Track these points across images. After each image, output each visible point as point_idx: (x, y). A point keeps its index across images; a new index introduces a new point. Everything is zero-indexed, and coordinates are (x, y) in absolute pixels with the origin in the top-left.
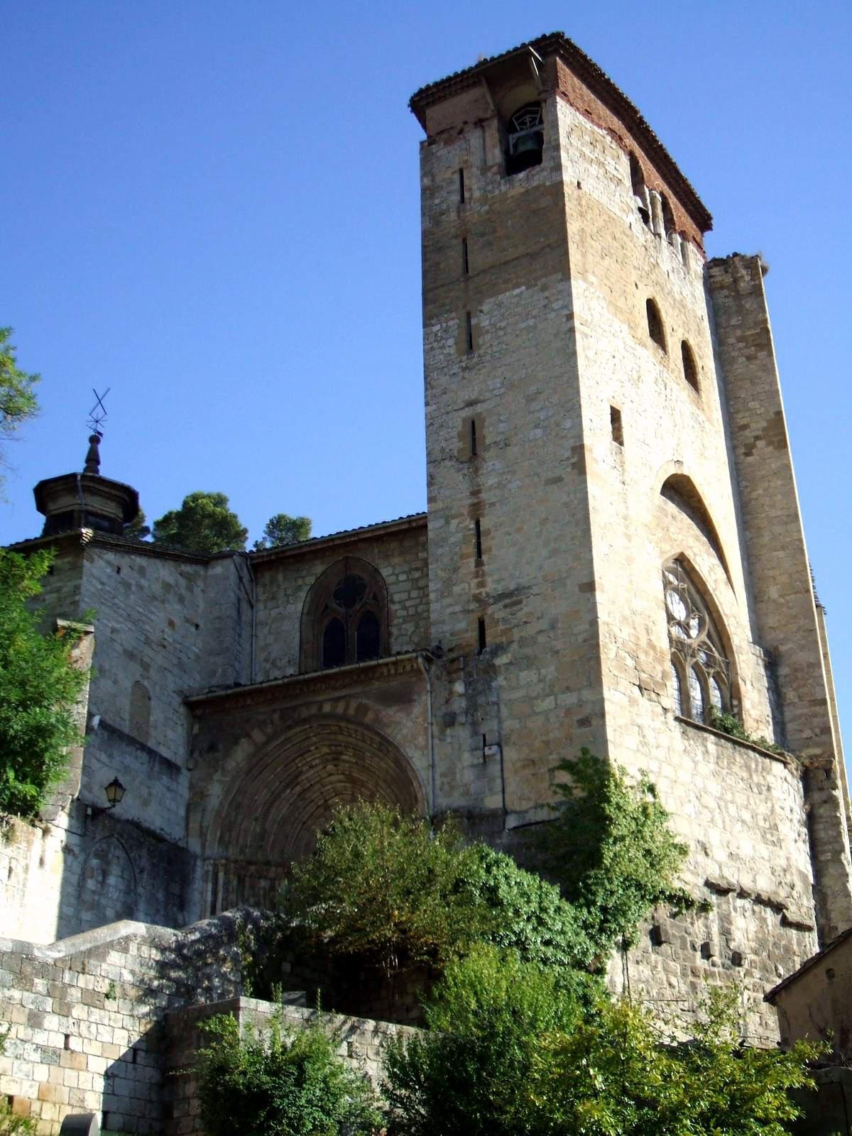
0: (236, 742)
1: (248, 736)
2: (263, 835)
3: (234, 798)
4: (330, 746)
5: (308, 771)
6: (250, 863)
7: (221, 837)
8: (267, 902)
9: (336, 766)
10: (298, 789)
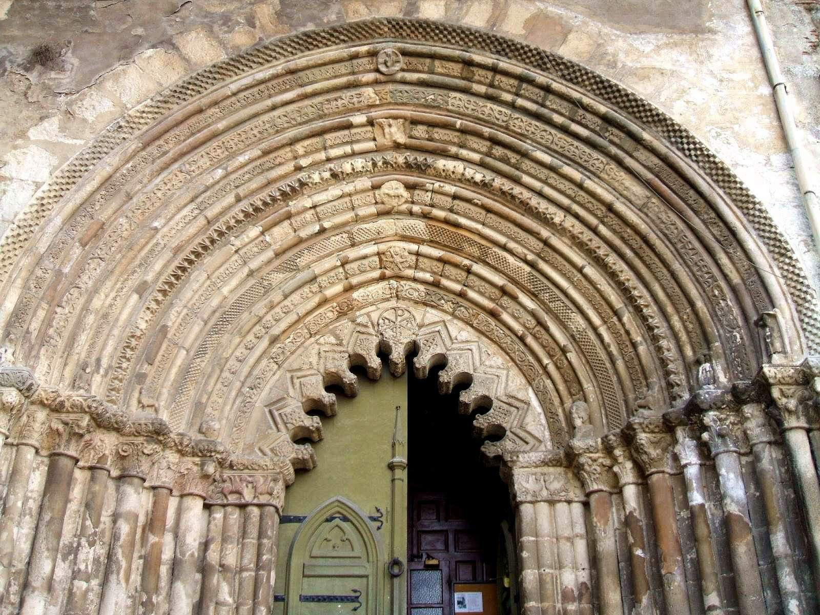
0: (127, 51)
1: (168, 43)
2: (149, 347)
3: (89, 200)
4: (415, 122)
5: (324, 185)
6: (101, 422)
7: (18, 315)
8: (138, 564)
9: (410, 187)
10: (282, 234)
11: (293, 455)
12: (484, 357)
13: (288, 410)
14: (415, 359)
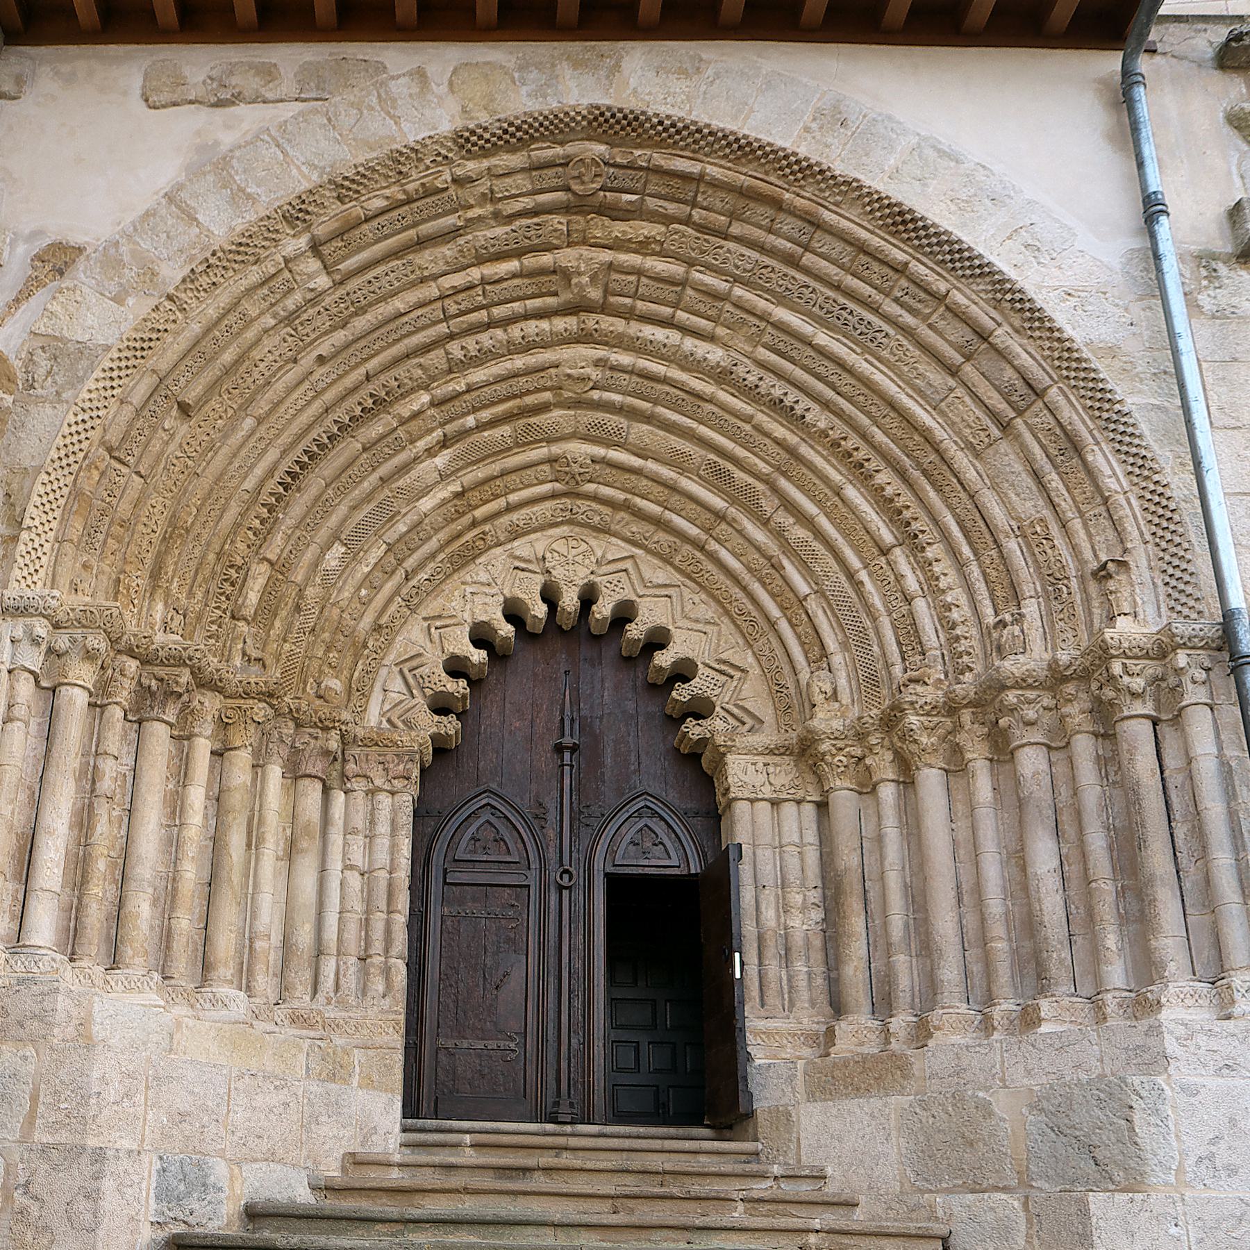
11: (434, 729)
12: (689, 606)
13: (425, 671)
14: (594, 608)
